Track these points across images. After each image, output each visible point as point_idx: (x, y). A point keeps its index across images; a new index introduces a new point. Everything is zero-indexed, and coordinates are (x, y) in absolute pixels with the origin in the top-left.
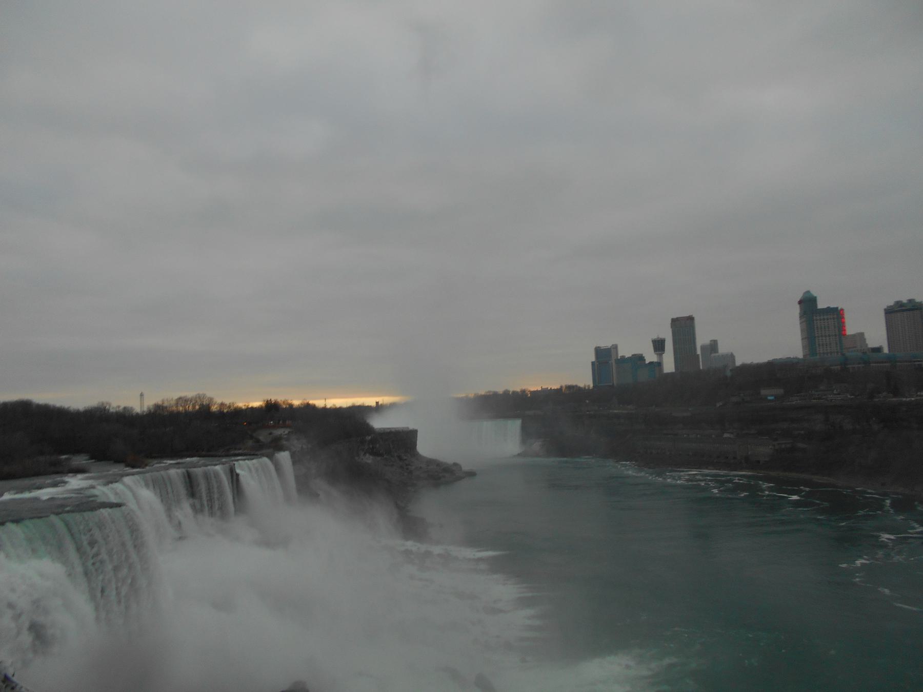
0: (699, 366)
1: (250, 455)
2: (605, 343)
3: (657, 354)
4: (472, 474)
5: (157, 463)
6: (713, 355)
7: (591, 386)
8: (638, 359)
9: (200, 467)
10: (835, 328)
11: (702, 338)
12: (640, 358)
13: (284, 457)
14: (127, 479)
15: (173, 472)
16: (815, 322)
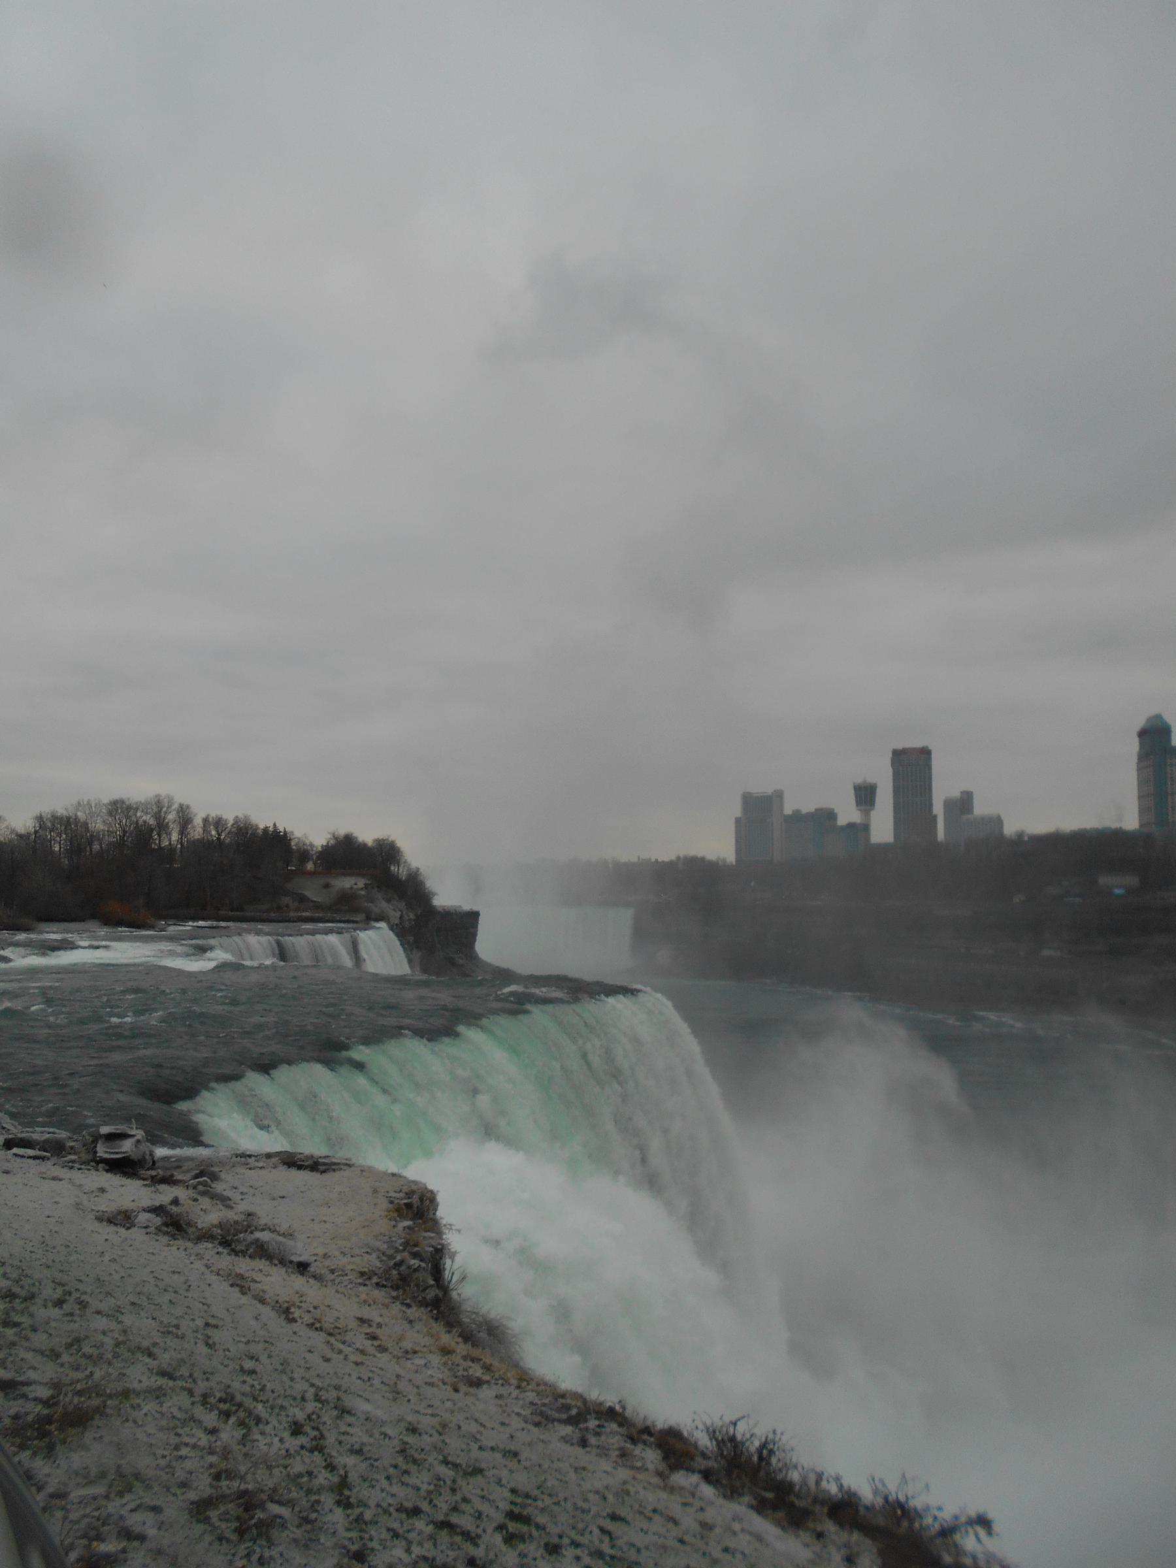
6: (965, 817)
9: (301, 935)
11: (943, 789)
12: (831, 815)
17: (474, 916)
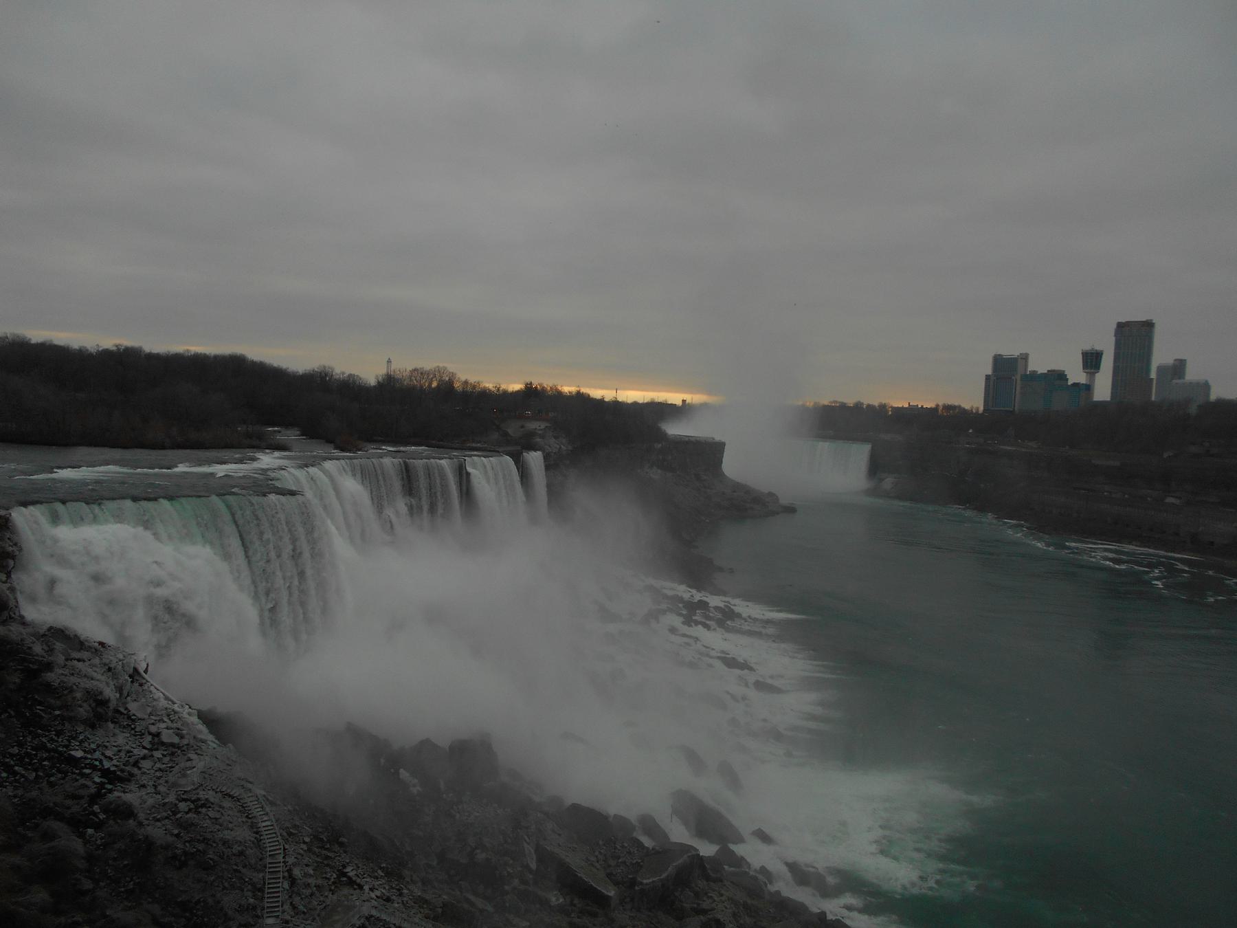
0: (1151, 397)
1: (490, 451)
2: (1010, 350)
3: (1085, 372)
4: (790, 510)
5: (374, 449)
7: (981, 409)
8: (1058, 377)
11: (1162, 355)
12: (1061, 376)
13: (535, 459)
14: (328, 465)
15: (387, 461)
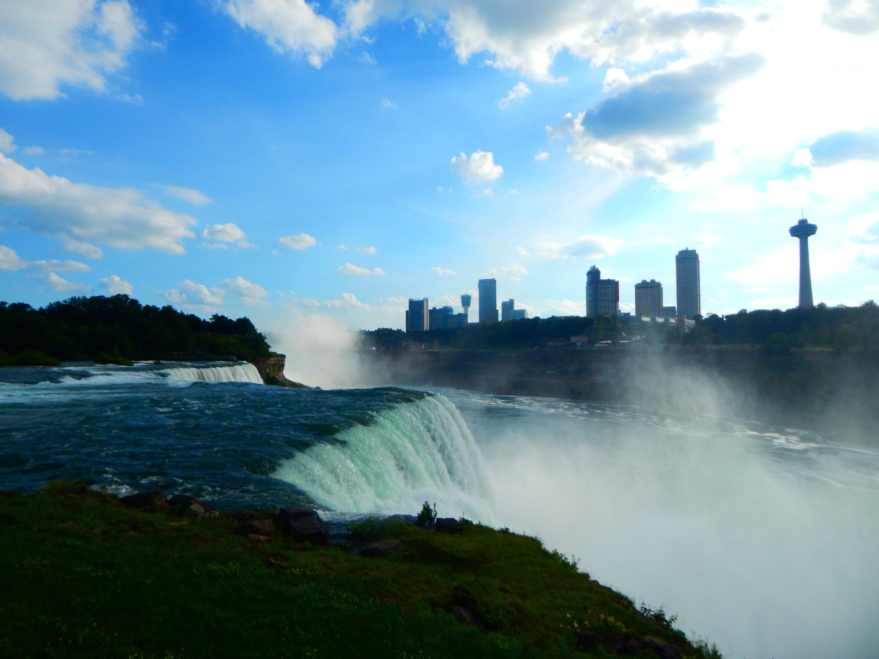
2: (418, 297)
7: (404, 329)
8: (447, 310)
10: (612, 295)
16: (599, 289)
17: (283, 356)
